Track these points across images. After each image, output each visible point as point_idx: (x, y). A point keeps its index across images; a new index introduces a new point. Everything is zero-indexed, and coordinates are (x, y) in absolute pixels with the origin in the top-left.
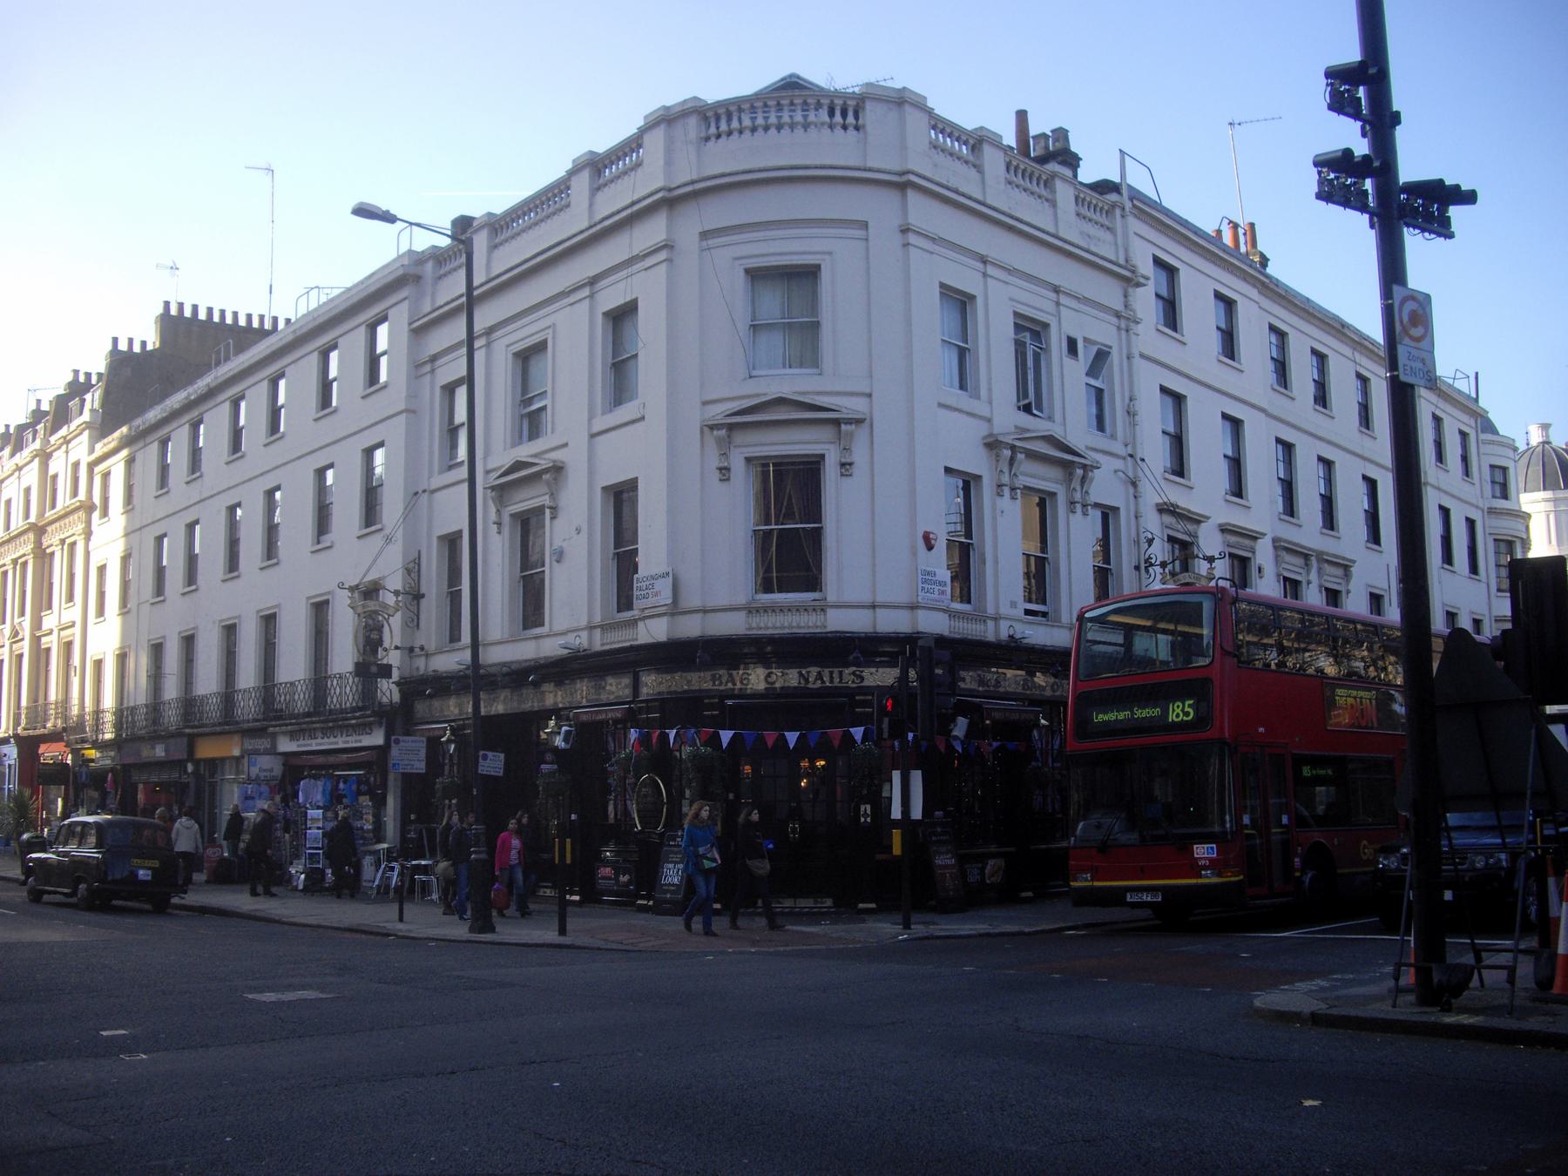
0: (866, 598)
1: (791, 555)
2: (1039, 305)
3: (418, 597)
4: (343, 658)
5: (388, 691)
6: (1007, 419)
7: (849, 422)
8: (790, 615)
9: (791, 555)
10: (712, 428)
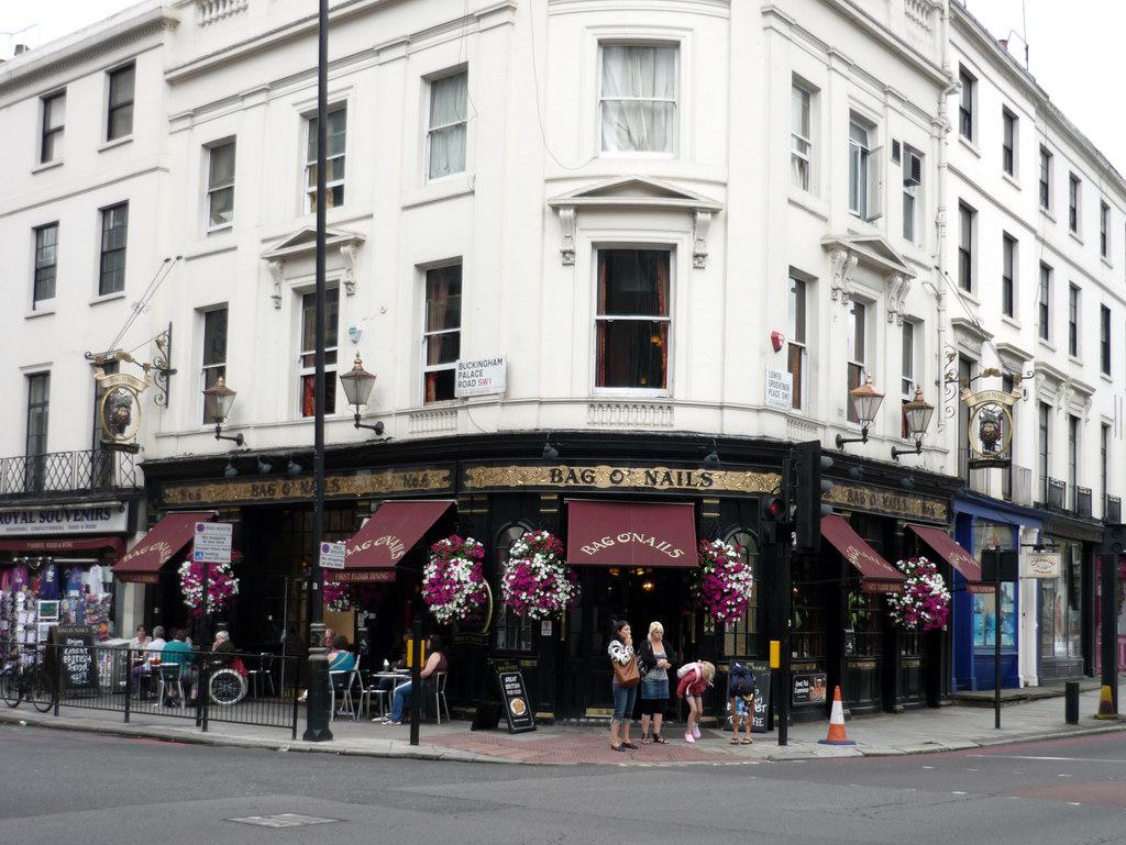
0: (716, 400)
1: (632, 351)
2: (871, 104)
3: (167, 372)
5: (127, 471)
6: (843, 224)
7: (704, 210)
8: (630, 411)
9: (632, 351)
10: (556, 208)
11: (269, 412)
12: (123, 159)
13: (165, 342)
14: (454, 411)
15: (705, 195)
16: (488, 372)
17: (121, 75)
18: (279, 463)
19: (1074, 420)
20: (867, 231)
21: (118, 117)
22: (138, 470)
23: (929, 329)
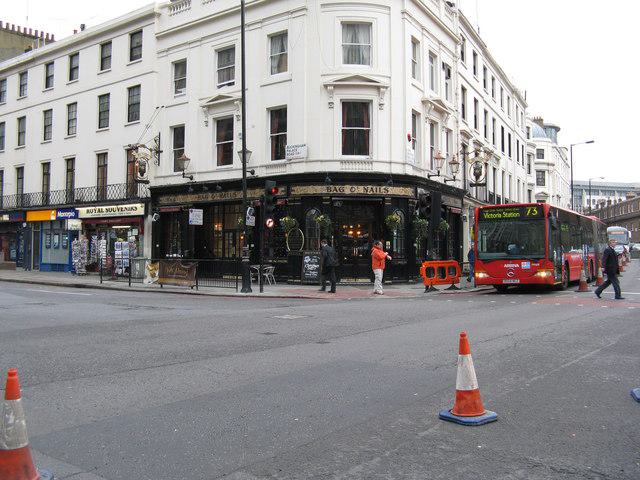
0: (388, 160)
1: (356, 140)
2: (435, 48)
3: (159, 152)
4: (117, 175)
5: (143, 191)
6: (429, 94)
7: (384, 87)
8: (356, 164)
9: (356, 140)
10: (326, 86)
11: (203, 164)
12: (137, 68)
13: (158, 140)
14: (285, 165)
15: (383, 81)
16: (299, 150)
17: (136, 35)
18: (212, 186)
19: (494, 169)
20: (436, 96)
21: (135, 53)
22: (149, 192)
23: (454, 133)
